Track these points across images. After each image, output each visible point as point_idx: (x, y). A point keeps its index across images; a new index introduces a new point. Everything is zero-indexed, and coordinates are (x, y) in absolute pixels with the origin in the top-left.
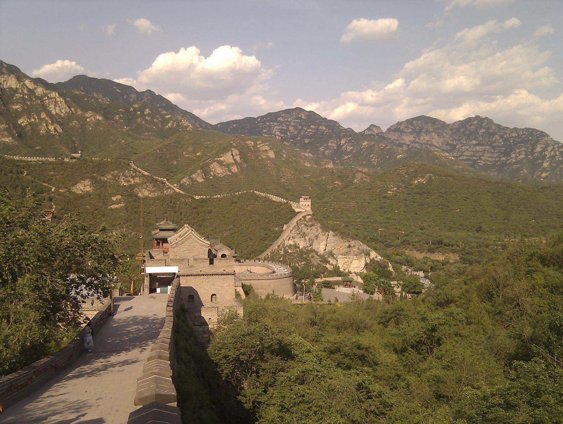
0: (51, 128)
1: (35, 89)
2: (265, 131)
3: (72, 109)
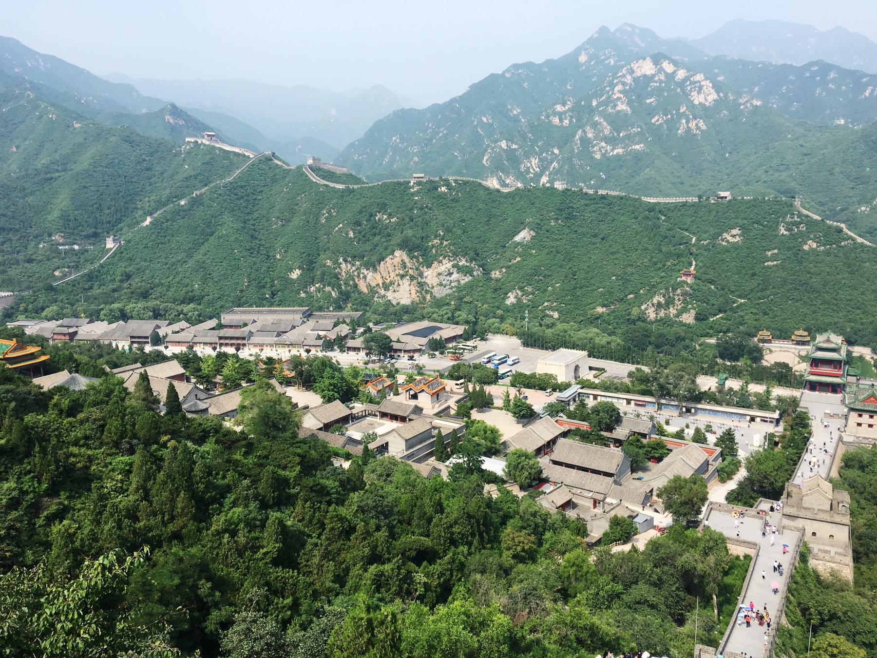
0: (692, 125)
1: (674, 72)
3: (721, 95)
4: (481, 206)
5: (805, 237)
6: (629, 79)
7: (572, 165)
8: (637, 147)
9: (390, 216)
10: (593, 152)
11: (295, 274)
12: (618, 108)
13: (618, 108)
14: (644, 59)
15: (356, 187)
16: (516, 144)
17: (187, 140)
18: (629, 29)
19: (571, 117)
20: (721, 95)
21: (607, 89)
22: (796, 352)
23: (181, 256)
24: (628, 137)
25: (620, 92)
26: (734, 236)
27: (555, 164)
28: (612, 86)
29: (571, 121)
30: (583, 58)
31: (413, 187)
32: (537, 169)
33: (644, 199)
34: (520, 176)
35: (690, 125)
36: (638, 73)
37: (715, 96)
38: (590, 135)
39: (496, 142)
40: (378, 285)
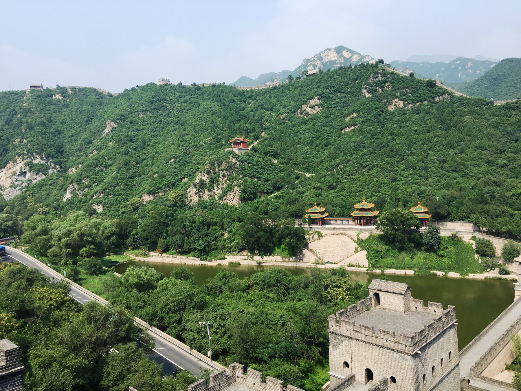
22: (354, 234)
26: (313, 107)
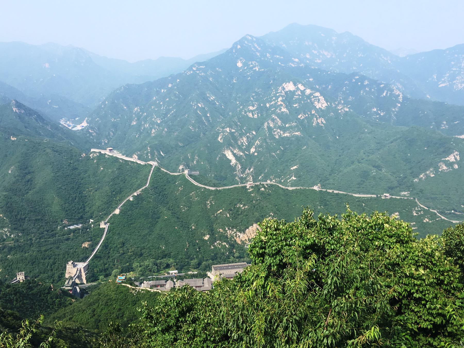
0: (319, 121)
1: (305, 90)
2: (453, 63)
4: (283, 198)
5: (424, 216)
6: (283, 93)
7: (267, 143)
8: (297, 133)
9: (244, 205)
10: (275, 135)
11: (207, 237)
12: (282, 110)
13: (282, 110)
14: (289, 83)
15: (221, 188)
16: (234, 129)
17: (92, 150)
18: (250, 38)
19: (258, 114)
20: (329, 104)
21: (274, 98)
23: (146, 232)
24: (291, 127)
25: (282, 101)
27: (257, 142)
28: (277, 98)
29: (258, 116)
30: (239, 64)
31: (249, 189)
32: (247, 143)
33: (354, 195)
34: (240, 148)
35: (318, 121)
36: (287, 90)
37: (326, 105)
38: (271, 125)
39: (223, 128)
40: (246, 240)
